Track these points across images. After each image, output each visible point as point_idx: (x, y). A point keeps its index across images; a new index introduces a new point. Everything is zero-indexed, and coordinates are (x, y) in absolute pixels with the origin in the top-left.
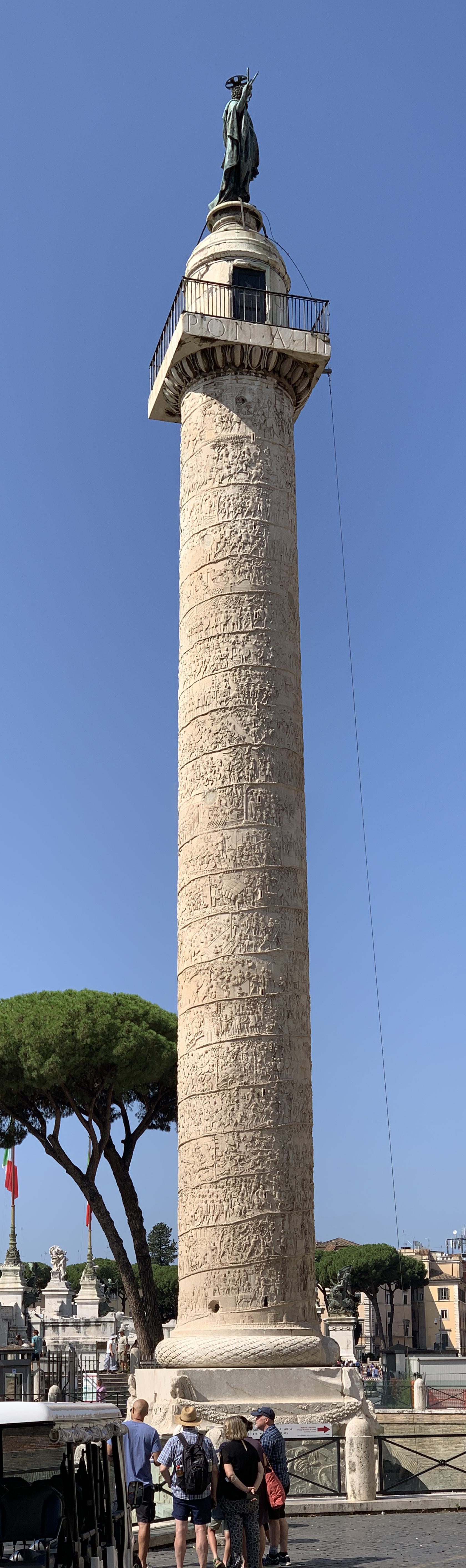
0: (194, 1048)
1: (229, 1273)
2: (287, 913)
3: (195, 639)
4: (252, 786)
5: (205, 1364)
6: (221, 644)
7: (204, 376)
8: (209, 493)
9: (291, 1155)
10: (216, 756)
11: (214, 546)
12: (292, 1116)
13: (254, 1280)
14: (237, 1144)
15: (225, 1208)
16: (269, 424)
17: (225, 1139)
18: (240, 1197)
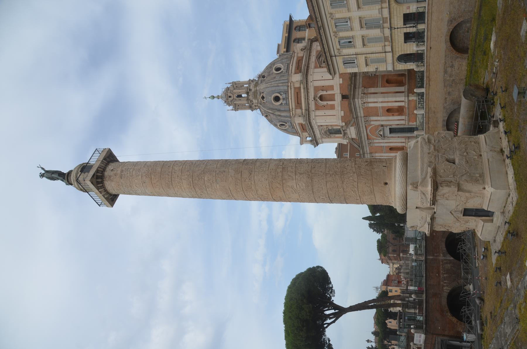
1: (374, 178)
5: (406, 178)
8: (133, 180)
10: (206, 179)
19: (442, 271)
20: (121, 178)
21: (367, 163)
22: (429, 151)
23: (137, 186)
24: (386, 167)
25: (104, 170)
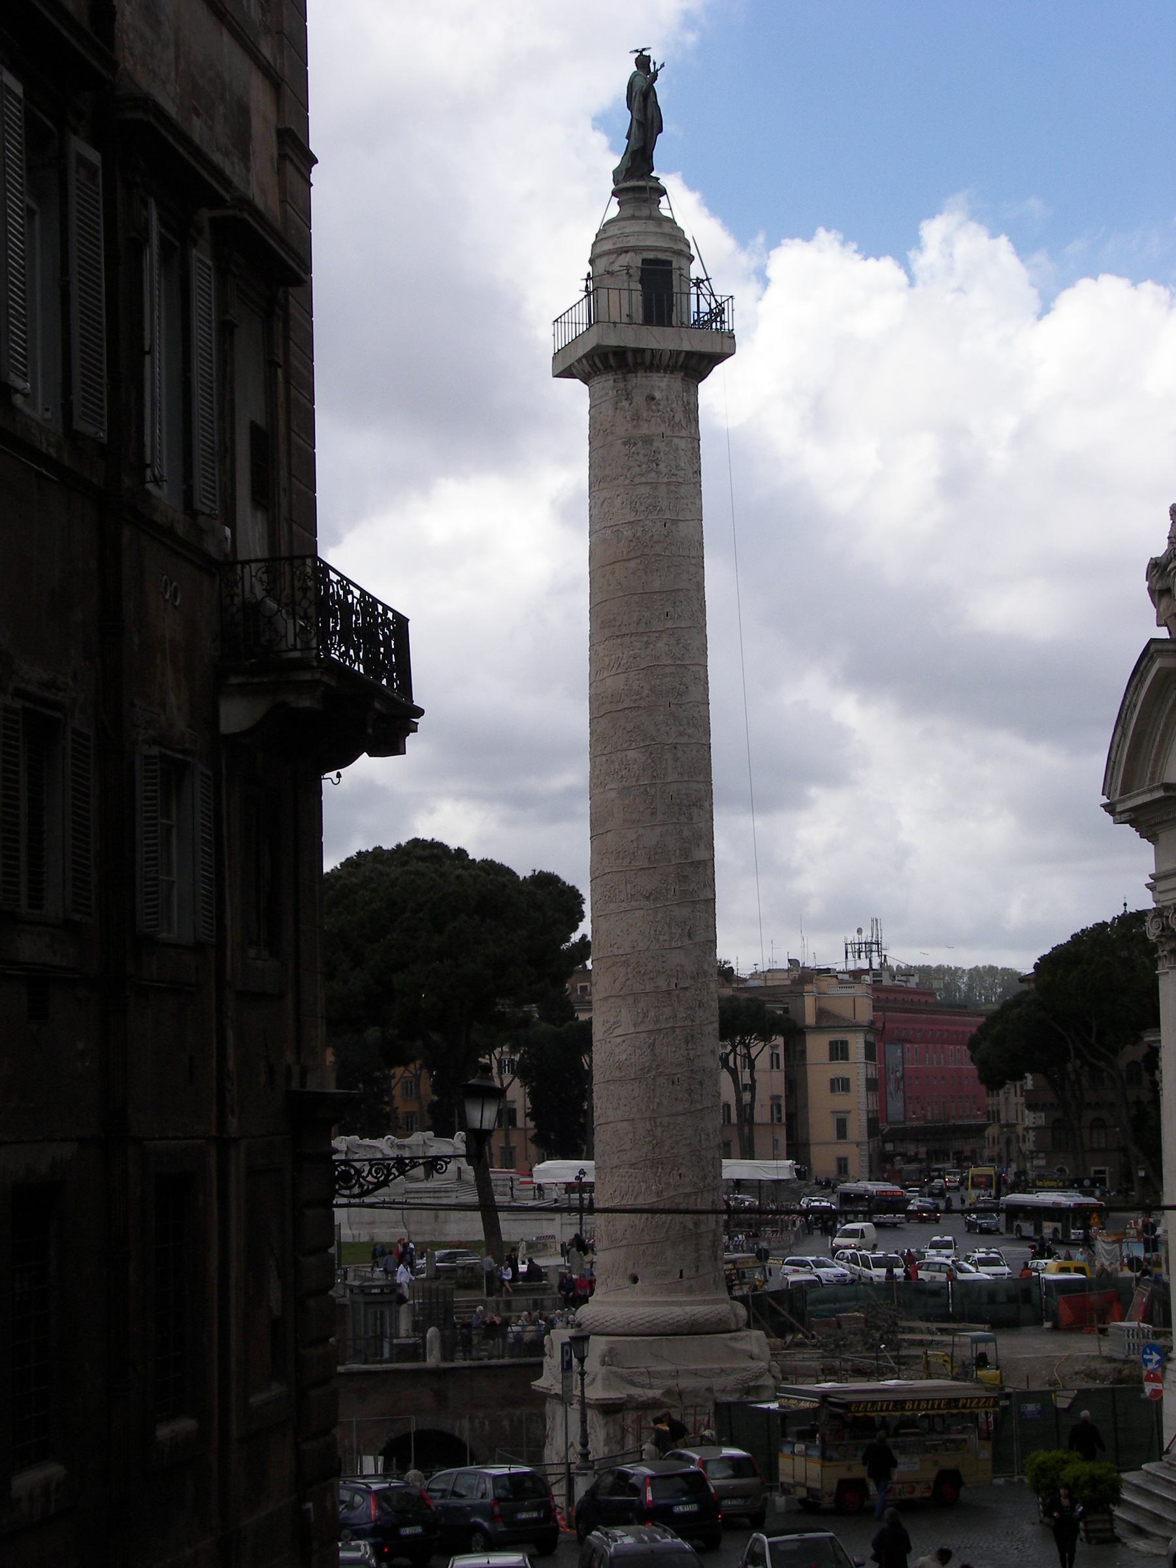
0: (610, 1035)
9: (703, 1136)
10: (631, 754)
19: (518, 1412)
21: (691, 1226)
22: (718, 1391)
23: (606, 503)
24: (681, 1277)
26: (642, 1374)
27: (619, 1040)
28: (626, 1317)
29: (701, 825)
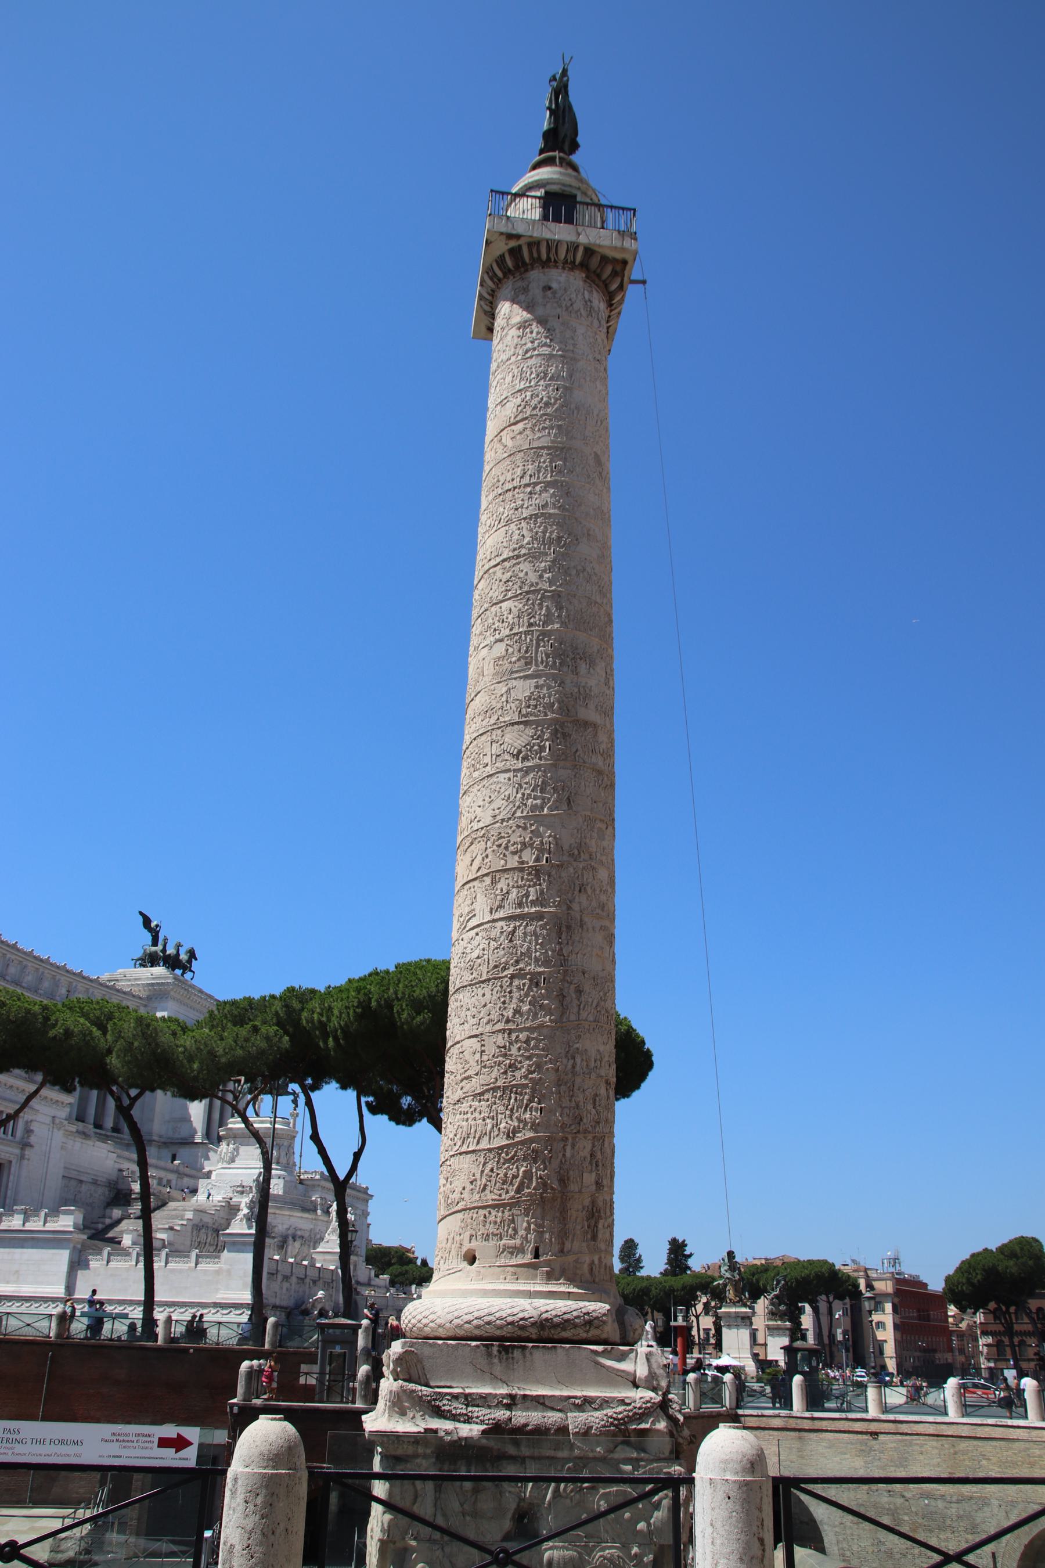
0: (465, 931)
1: (490, 1213)
2: (582, 772)
3: (490, 497)
4: (544, 634)
6: (517, 496)
7: (513, 274)
9: (578, 1060)
11: (515, 410)
12: (581, 1012)
13: (522, 1223)
14: (508, 1044)
15: (489, 1127)
16: (576, 306)
17: (493, 1039)
18: (508, 1112)
20: (519, 328)
25: (546, 264)
26: (455, 1397)
27: (473, 933)
28: (447, 1310)
29: (592, 682)
